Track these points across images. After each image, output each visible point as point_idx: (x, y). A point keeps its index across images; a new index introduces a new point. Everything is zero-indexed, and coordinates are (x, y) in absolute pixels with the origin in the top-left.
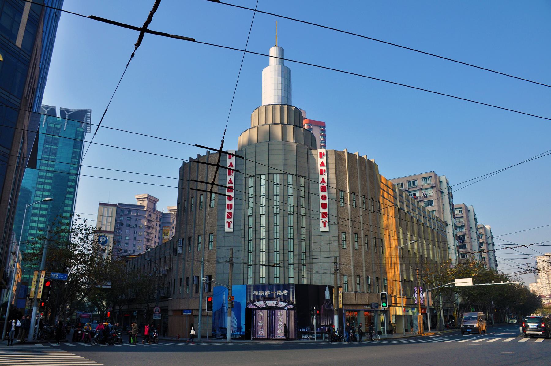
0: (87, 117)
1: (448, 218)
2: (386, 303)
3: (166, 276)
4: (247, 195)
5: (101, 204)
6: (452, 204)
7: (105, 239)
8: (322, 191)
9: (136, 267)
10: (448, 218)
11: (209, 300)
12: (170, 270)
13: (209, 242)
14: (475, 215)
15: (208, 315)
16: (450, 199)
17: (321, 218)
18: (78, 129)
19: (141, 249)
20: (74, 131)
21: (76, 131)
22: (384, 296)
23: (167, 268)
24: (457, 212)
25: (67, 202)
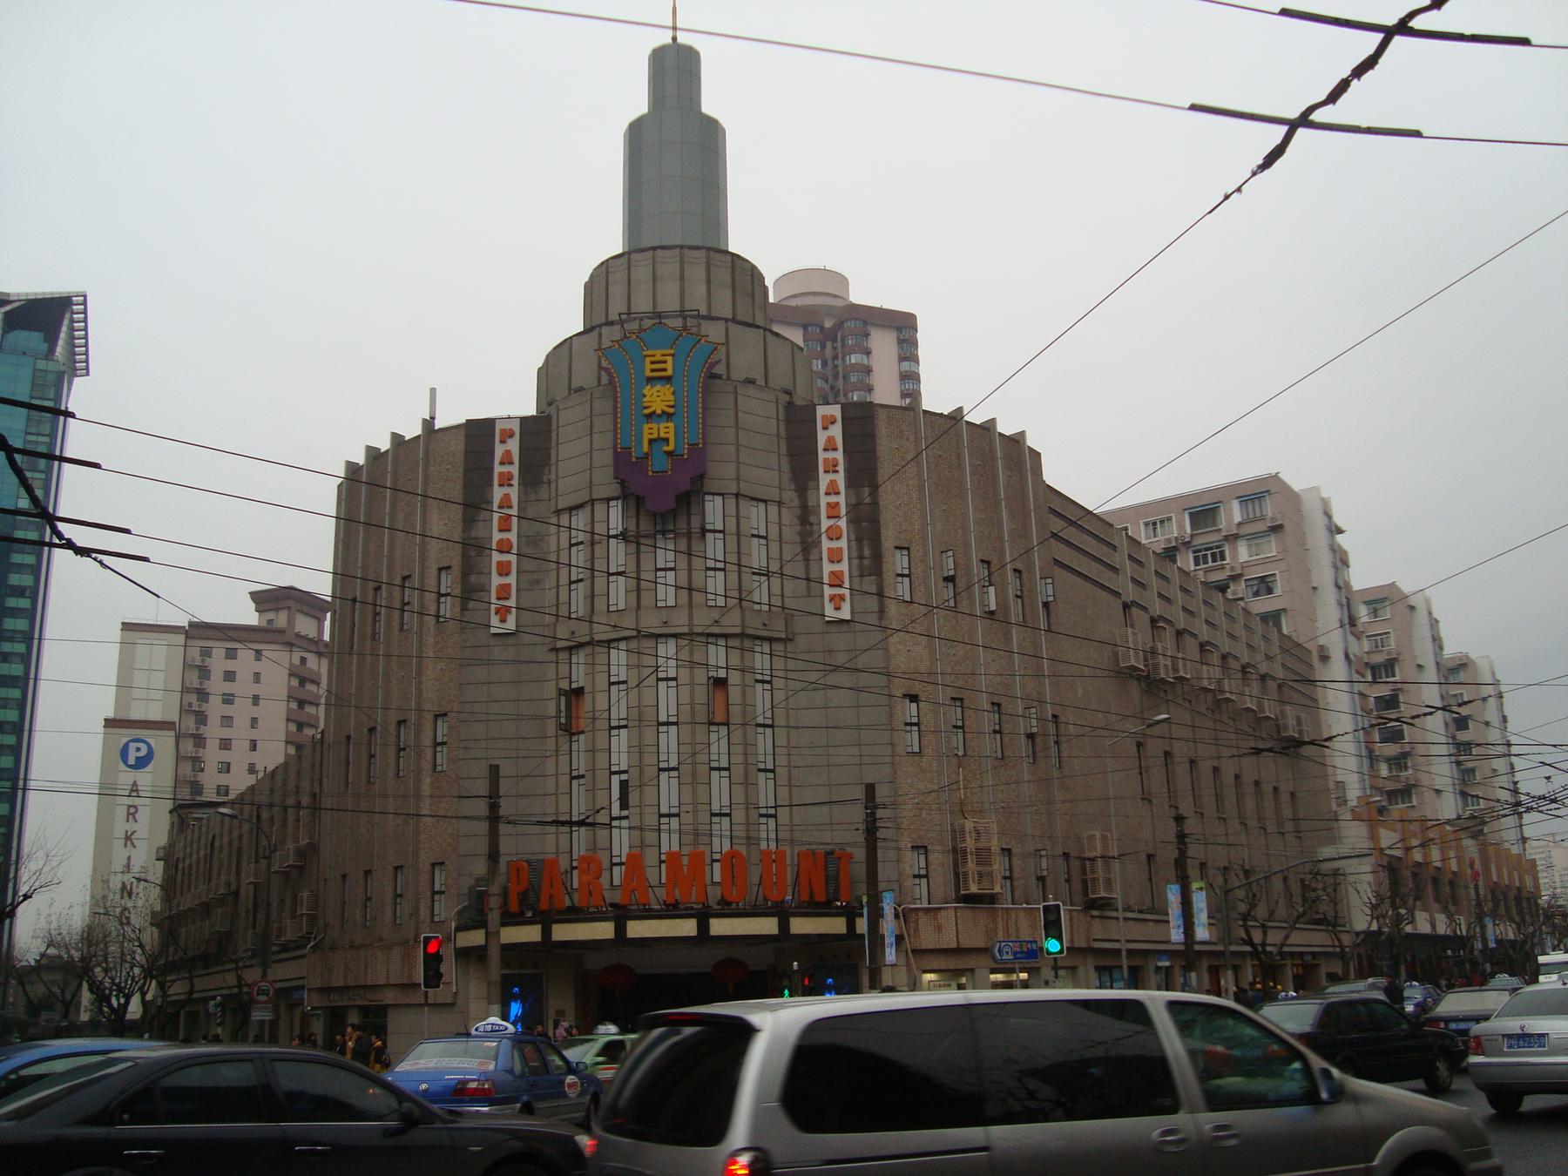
0: (72, 321)
1: (1335, 641)
2: (1060, 939)
3: (301, 868)
4: (564, 571)
5: (127, 627)
6: (1341, 586)
7: (143, 753)
8: (840, 549)
9: (217, 844)
10: (1335, 641)
11: (432, 949)
12: (308, 854)
13: (436, 744)
14: (1434, 623)
15: (426, 1004)
16: (1336, 568)
17: (493, 600)
18: (41, 364)
19: (240, 782)
20: (26, 373)
21: (35, 370)
22: (1052, 917)
23: (304, 842)
24: (1363, 613)
25: (9, 623)
